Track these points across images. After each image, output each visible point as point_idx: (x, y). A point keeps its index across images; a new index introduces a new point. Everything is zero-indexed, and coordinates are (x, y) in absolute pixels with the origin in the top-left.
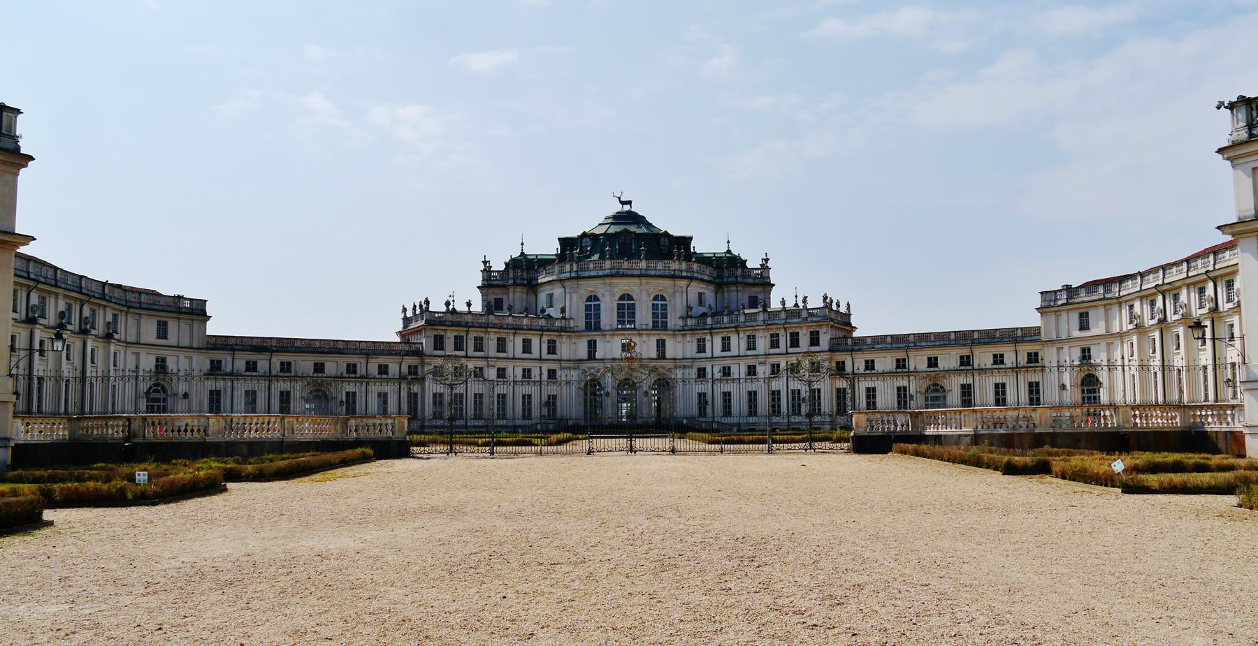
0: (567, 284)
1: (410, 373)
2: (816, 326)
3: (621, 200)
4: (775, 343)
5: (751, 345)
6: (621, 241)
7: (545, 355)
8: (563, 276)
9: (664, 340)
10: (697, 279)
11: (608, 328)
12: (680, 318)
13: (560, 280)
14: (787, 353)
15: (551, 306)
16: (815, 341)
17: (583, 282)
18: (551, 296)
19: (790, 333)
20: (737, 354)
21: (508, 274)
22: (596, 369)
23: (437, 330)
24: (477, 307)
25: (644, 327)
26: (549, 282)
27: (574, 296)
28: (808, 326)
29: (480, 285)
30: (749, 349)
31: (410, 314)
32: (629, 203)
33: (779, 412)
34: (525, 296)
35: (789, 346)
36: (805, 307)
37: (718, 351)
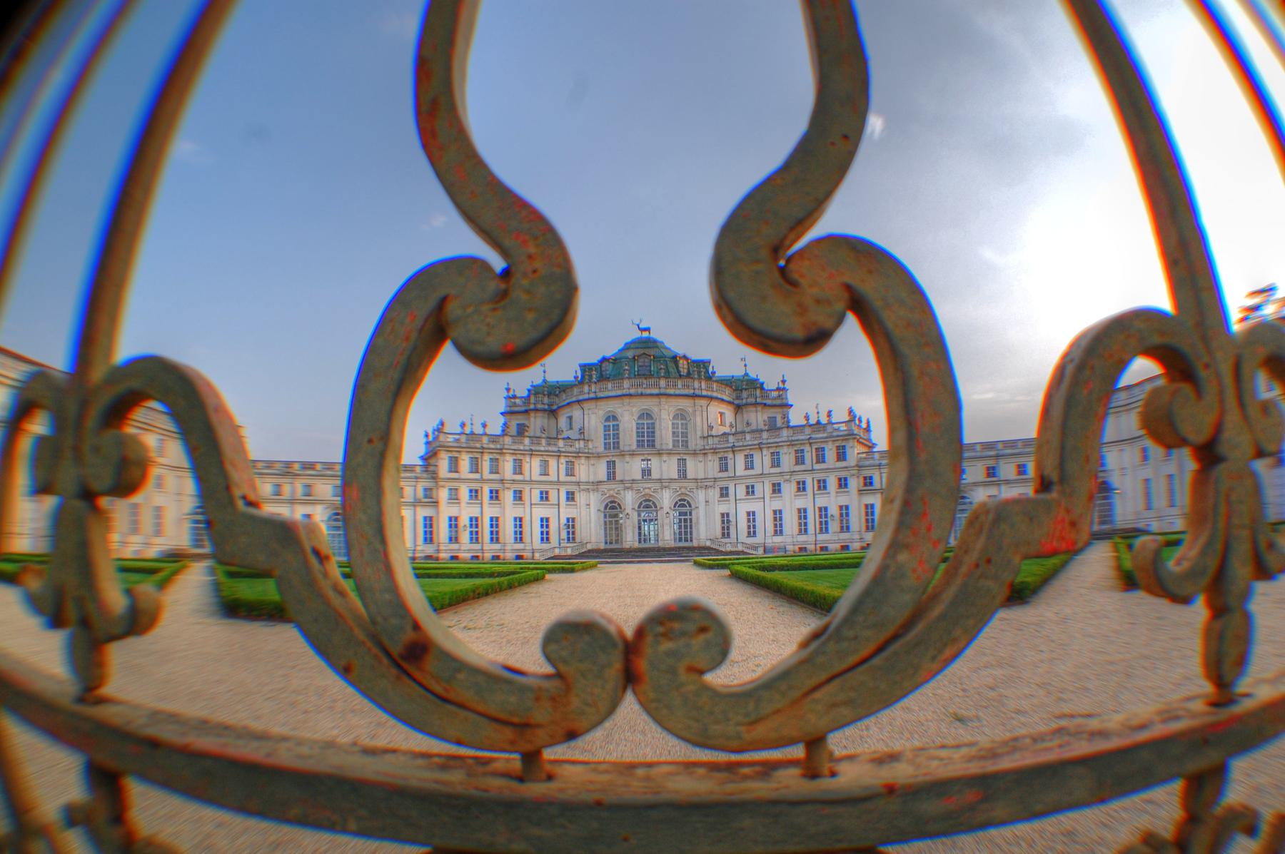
0: (586, 405)
1: (426, 497)
2: (843, 440)
3: (640, 326)
4: (800, 460)
5: (776, 463)
6: (640, 364)
7: (563, 478)
8: (581, 398)
9: (685, 459)
10: (717, 398)
11: (627, 448)
12: (701, 437)
13: (578, 402)
14: (813, 470)
15: (571, 428)
16: (841, 456)
17: (602, 404)
18: (570, 418)
19: (816, 449)
20: (761, 472)
21: (530, 400)
22: (616, 490)
23: (451, 451)
24: (495, 427)
25: (664, 447)
26: (568, 404)
27: (593, 417)
28: (834, 441)
29: (503, 411)
30: (773, 466)
31: (431, 438)
32: (647, 330)
33: (806, 530)
34: (546, 421)
35: (814, 461)
36: (830, 423)
37: (740, 470)
